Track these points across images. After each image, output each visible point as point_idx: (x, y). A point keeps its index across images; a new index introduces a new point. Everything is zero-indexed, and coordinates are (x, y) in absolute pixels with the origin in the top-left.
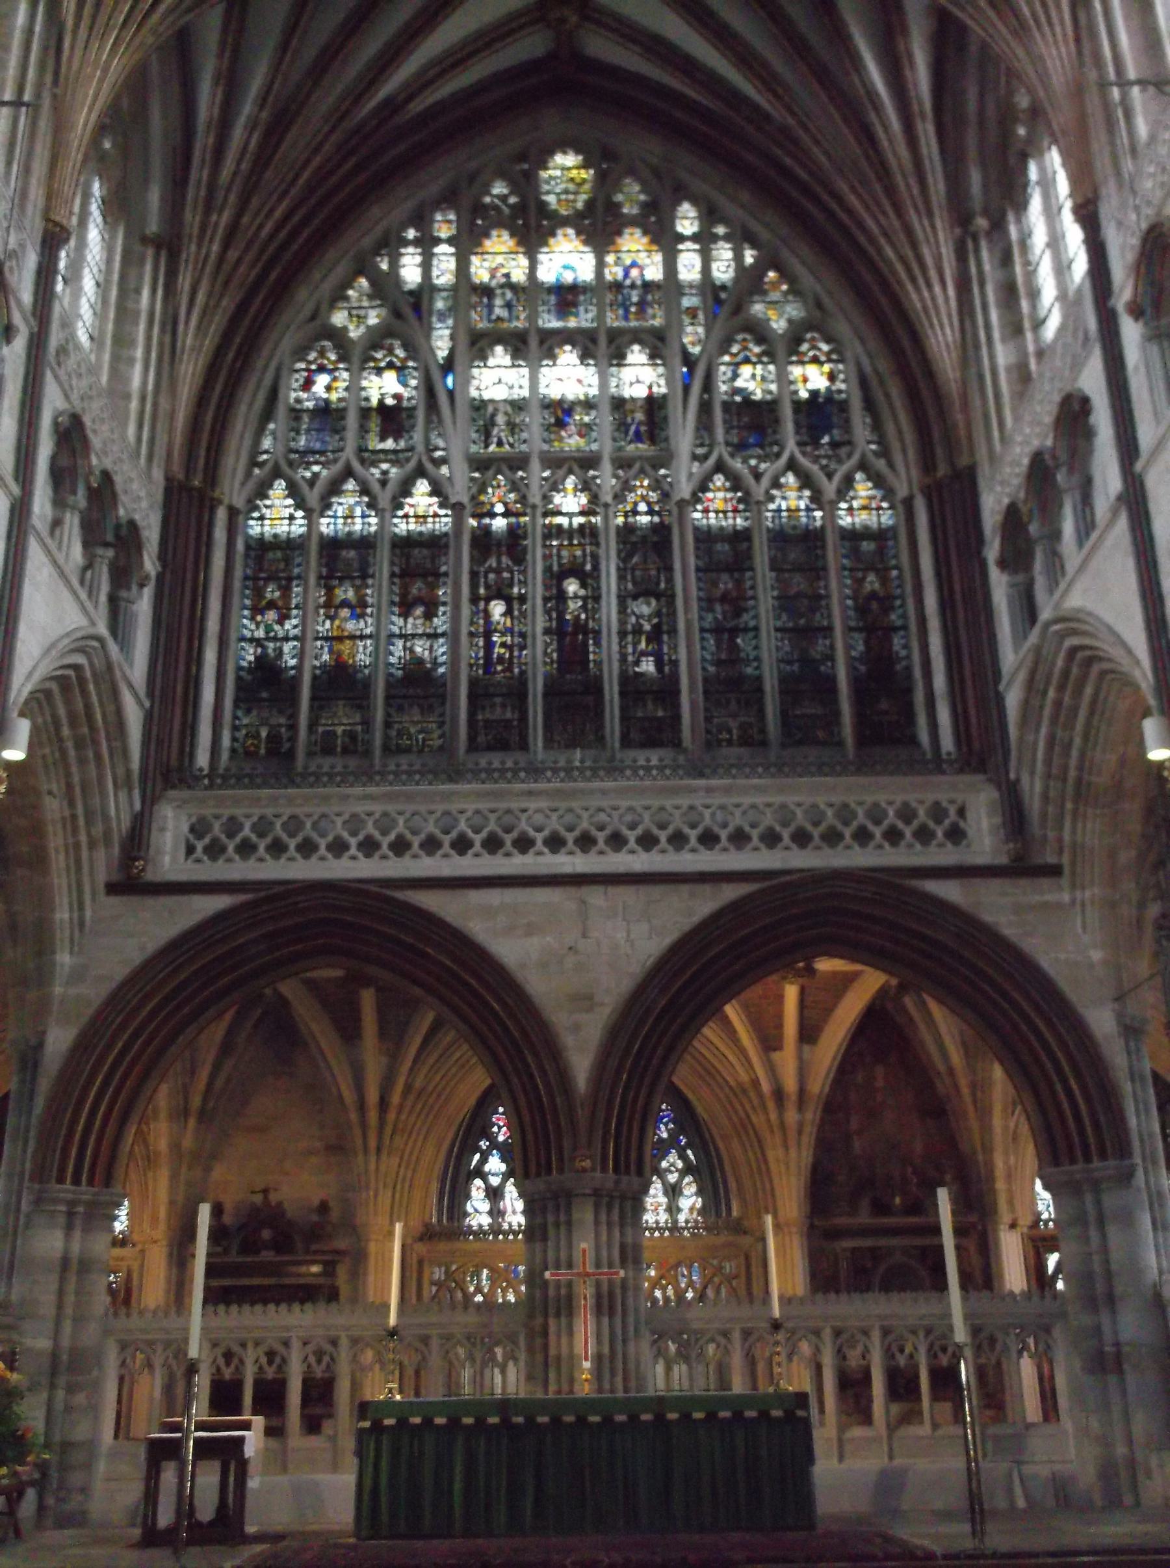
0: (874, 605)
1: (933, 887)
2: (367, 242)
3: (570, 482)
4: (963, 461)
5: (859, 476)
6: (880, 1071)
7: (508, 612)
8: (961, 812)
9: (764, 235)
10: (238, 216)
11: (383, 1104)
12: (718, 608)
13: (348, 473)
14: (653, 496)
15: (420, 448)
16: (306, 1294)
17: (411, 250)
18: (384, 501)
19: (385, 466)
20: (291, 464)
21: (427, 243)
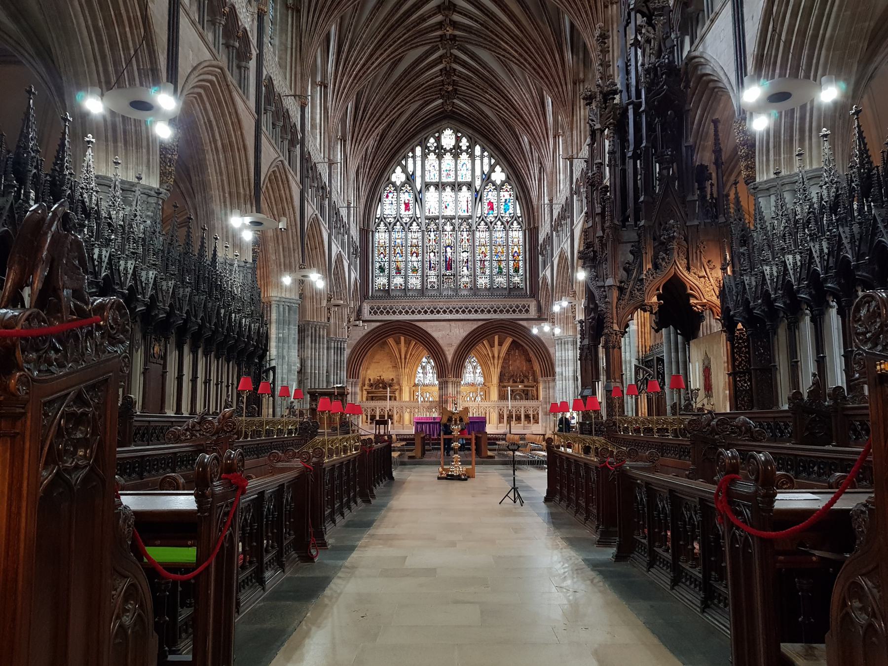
2: (400, 158)
3: (448, 223)
5: (515, 222)
9: (496, 157)
13: (398, 220)
14: (468, 227)
18: (406, 230)
21: (414, 157)
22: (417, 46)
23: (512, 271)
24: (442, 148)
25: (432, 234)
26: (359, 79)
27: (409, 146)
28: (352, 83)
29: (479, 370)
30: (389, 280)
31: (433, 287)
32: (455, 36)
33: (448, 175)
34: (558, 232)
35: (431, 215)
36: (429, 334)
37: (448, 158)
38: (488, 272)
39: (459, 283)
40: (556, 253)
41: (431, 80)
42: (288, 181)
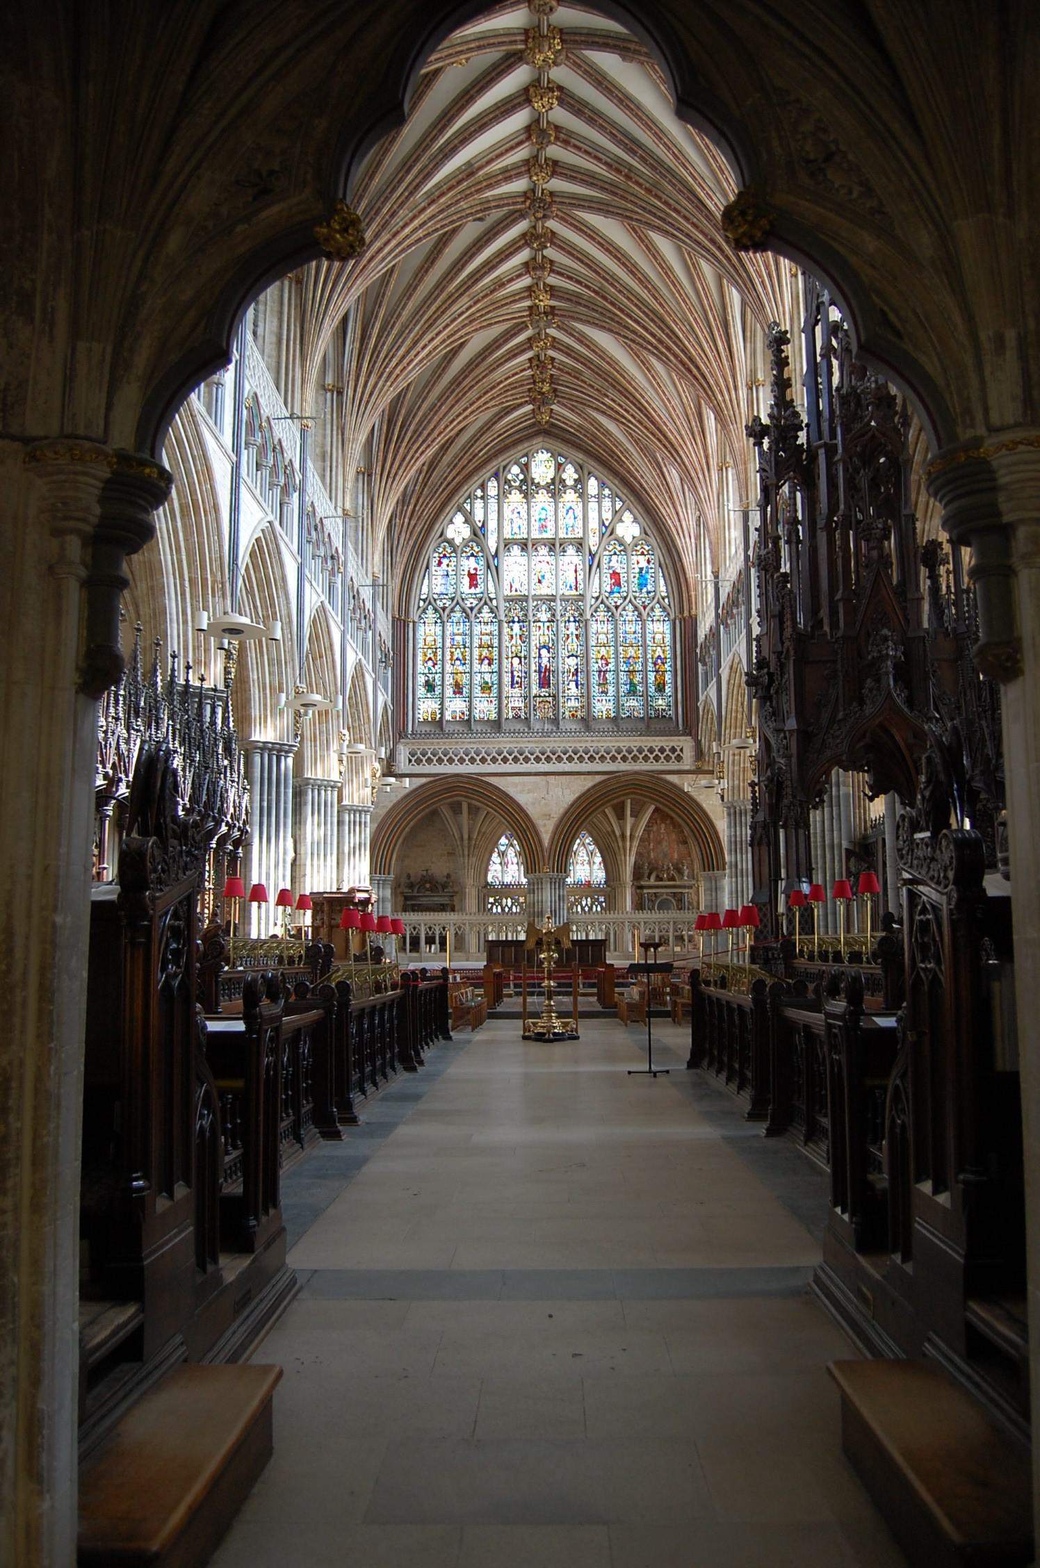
0: (659, 661)
1: (670, 778)
2: (461, 501)
3: (544, 607)
4: (693, 612)
5: (658, 606)
6: (663, 826)
7: (521, 663)
8: (681, 750)
9: (624, 497)
10: (415, 506)
11: (470, 838)
12: (599, 661)
15: (486, 595)
16: (442, 908)
17: (479, 500)
19: (472, 600)
20: (435, 600)
22: (491, 324)
23: (652, 689)
24: (533, 483)
25: (516, 627)
26: (395, 380)
27: (477, 480)
28: (384, 386)
29: (598, 859)
30: (442, 704)
31: (517, 717)
32: (553, 308)
33: (543, 528)
34: (727, 626)
35: (514, 593)
36: (511, 798)
37: (542, 498)
38: (611, 689)
39: (562, 710)
40: (725, 664)
41: (513, 375)
42: (279, 553)
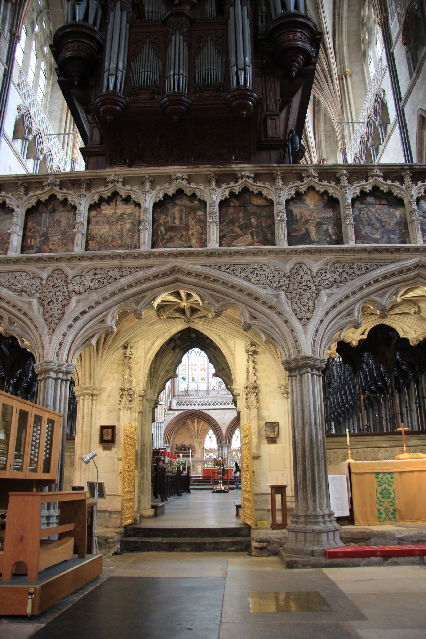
11: (198, 432)
